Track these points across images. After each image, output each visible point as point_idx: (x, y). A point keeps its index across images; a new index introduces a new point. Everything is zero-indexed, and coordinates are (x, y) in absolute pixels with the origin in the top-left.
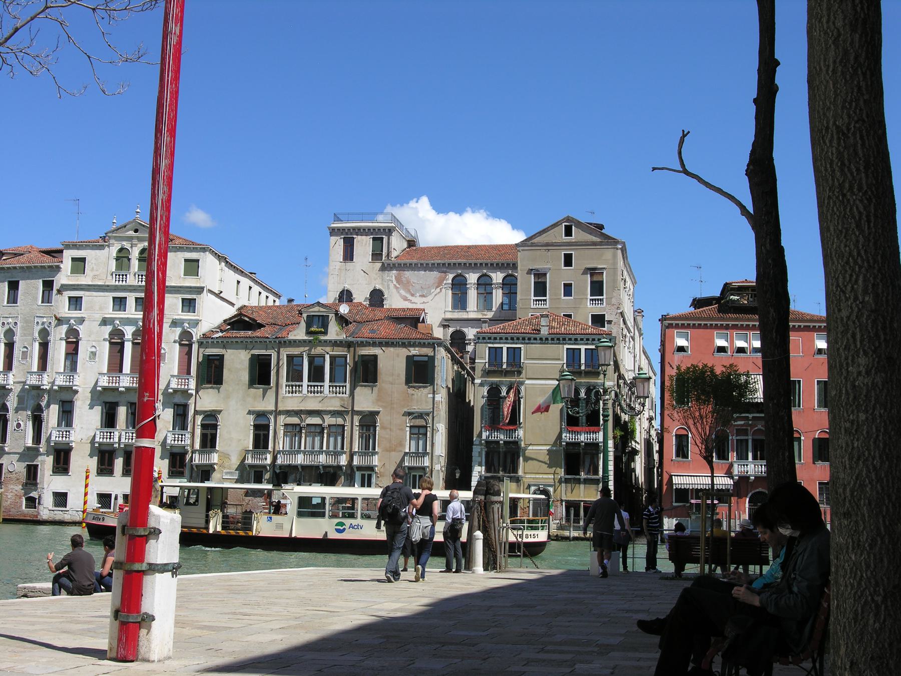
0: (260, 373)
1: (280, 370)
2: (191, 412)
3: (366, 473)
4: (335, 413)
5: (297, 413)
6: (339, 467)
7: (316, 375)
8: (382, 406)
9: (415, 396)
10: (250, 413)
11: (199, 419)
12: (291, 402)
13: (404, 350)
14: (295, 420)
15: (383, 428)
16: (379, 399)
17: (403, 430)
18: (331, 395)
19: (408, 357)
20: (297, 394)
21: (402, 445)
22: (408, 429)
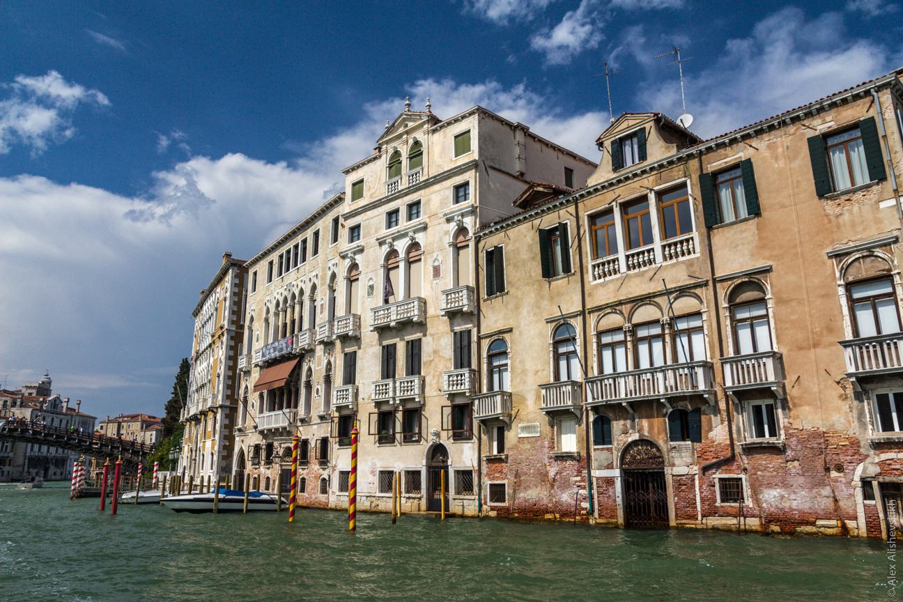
0: (553, 255)
1: (583, 243)
2: (474, 338)
3: (764, 403)
4: (682, 291)
5: (614, 307)
6: (697, 398)
7: (637, 236)
8: (770, 258)
9: (846, 217)
10: (549, 321)
11: (485, 344)
12: (603, 291)
13: (803, 130)
14: (614, 320)
15: (780, 301)
16: (763, 244)
17: (830, 295)
18: (669, 262)
19: (810, 140)
20: (614, 277)
21: (831, 328)
22: (841, 291)
